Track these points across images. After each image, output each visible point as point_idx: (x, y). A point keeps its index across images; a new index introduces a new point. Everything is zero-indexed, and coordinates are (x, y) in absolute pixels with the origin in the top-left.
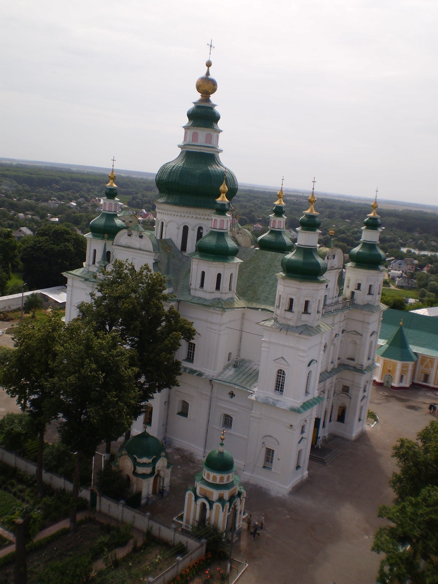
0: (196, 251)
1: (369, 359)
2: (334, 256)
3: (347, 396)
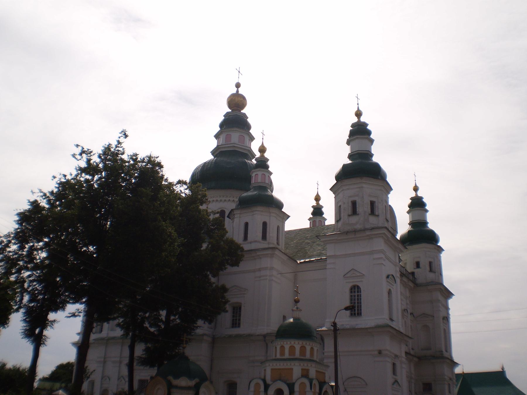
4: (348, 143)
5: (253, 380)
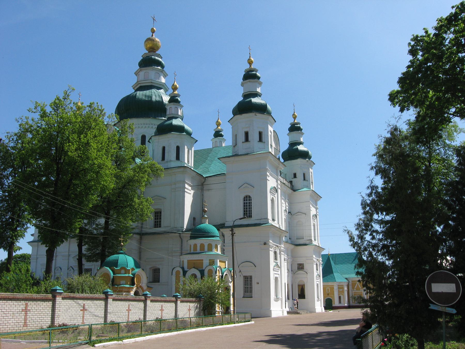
4: (242, 85)
5: (174, 268)
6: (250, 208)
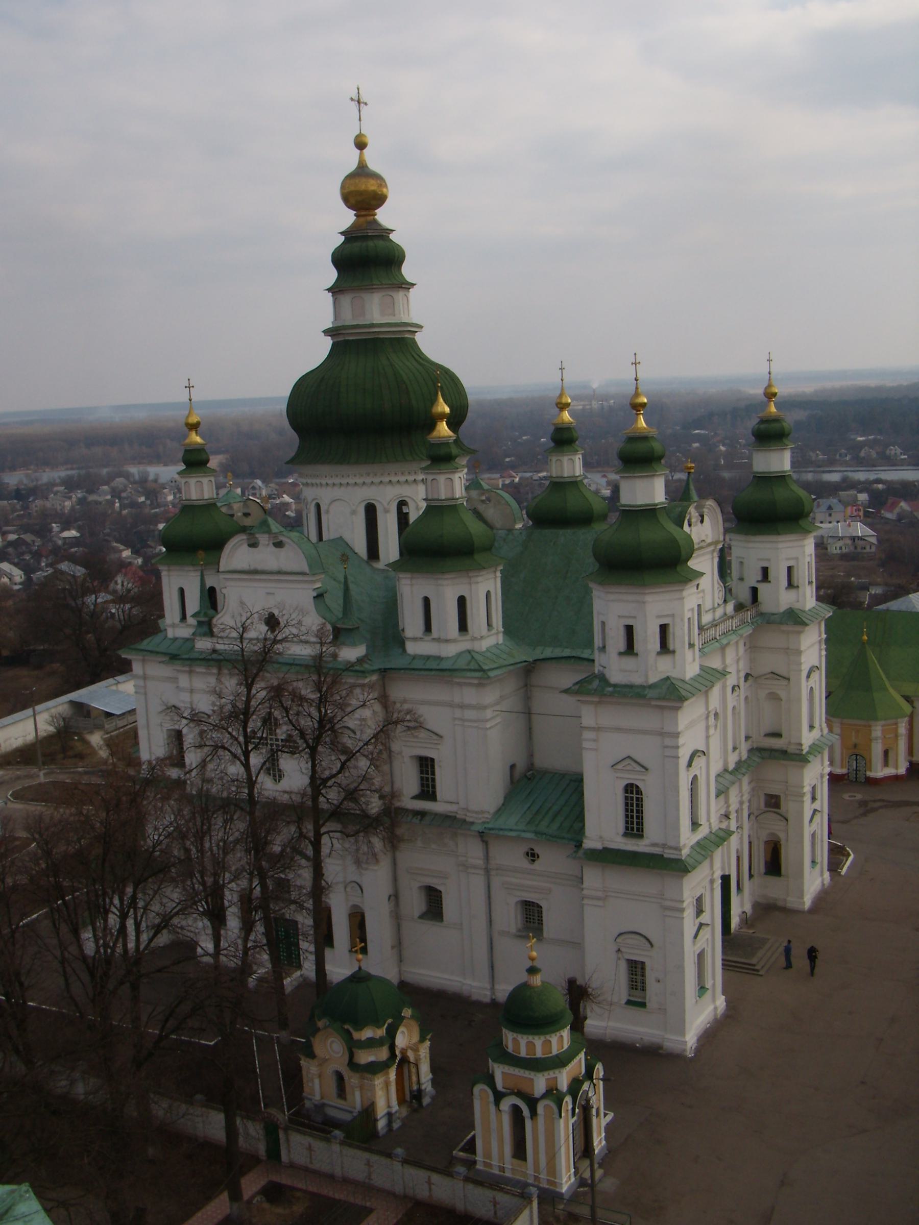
0: (401, 554)
1: (811, 727)
2: (702, 517)
3: (779, 817)
6: (640, 812)
